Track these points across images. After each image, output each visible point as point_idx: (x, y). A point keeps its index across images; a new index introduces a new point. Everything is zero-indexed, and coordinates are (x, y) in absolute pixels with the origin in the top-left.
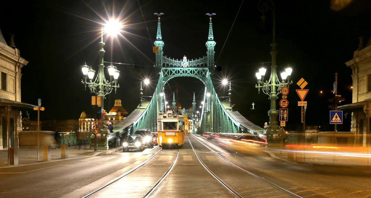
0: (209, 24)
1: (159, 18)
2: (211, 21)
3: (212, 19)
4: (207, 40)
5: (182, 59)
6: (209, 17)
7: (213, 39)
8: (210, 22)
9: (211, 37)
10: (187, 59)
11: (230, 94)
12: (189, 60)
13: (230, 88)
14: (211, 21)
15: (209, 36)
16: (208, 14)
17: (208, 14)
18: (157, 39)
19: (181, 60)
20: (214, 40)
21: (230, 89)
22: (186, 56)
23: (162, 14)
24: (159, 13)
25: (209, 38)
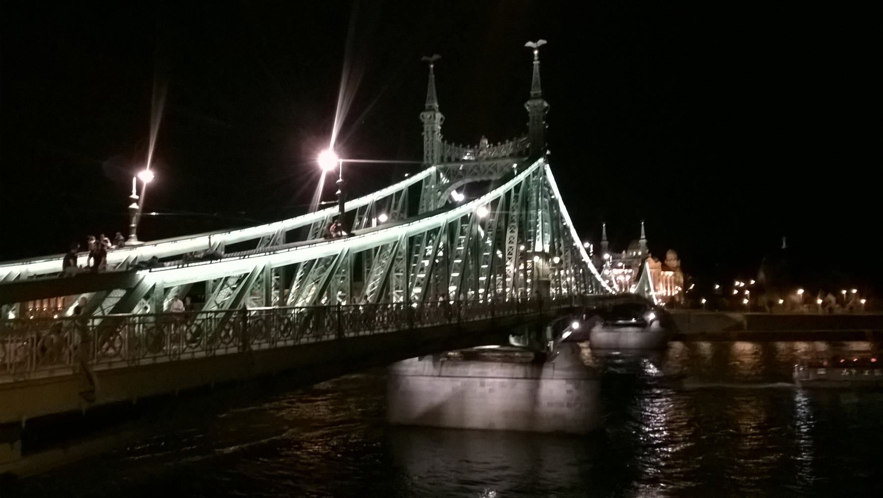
0: (533, 64)
1: (432, 66)
2: (536, 58)
3: (539, 55)
4: (528, 97)
5: (478, 143)
6: (532, 49)
7: (540, 95)
8: (534, 60)
9: (536, 91)
10: (489, 143)
11: (339, 192)
12: (492, 145)
13: (340, 176)
14: (536, 58)
15: (532, 89)
16: (530, 44)
17: (530, 44)
18: (426, 108)
19: (476, 147)
20: (544, 97)
21: (340, 180)
22: (487, 137)
23: (436, 57)
24: (431, 56)
25: (532, 93)
